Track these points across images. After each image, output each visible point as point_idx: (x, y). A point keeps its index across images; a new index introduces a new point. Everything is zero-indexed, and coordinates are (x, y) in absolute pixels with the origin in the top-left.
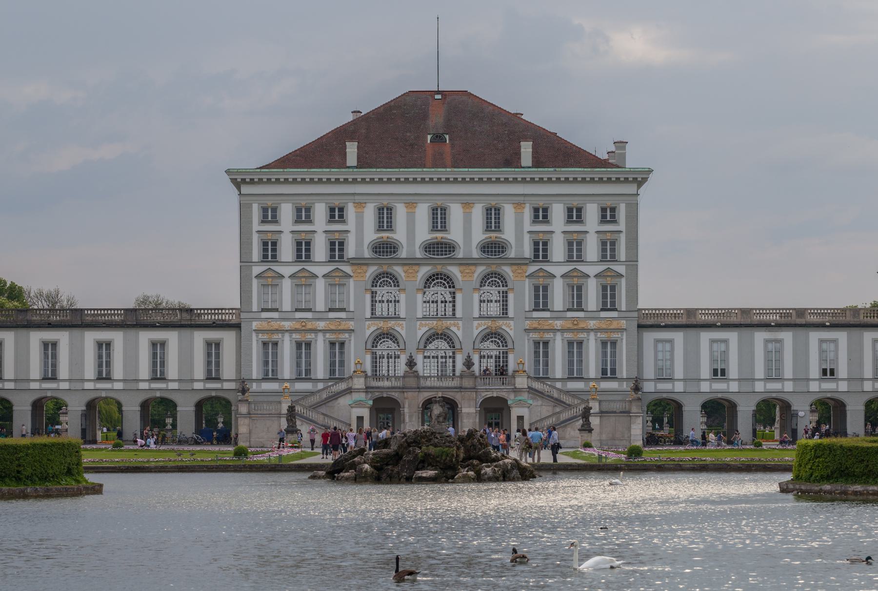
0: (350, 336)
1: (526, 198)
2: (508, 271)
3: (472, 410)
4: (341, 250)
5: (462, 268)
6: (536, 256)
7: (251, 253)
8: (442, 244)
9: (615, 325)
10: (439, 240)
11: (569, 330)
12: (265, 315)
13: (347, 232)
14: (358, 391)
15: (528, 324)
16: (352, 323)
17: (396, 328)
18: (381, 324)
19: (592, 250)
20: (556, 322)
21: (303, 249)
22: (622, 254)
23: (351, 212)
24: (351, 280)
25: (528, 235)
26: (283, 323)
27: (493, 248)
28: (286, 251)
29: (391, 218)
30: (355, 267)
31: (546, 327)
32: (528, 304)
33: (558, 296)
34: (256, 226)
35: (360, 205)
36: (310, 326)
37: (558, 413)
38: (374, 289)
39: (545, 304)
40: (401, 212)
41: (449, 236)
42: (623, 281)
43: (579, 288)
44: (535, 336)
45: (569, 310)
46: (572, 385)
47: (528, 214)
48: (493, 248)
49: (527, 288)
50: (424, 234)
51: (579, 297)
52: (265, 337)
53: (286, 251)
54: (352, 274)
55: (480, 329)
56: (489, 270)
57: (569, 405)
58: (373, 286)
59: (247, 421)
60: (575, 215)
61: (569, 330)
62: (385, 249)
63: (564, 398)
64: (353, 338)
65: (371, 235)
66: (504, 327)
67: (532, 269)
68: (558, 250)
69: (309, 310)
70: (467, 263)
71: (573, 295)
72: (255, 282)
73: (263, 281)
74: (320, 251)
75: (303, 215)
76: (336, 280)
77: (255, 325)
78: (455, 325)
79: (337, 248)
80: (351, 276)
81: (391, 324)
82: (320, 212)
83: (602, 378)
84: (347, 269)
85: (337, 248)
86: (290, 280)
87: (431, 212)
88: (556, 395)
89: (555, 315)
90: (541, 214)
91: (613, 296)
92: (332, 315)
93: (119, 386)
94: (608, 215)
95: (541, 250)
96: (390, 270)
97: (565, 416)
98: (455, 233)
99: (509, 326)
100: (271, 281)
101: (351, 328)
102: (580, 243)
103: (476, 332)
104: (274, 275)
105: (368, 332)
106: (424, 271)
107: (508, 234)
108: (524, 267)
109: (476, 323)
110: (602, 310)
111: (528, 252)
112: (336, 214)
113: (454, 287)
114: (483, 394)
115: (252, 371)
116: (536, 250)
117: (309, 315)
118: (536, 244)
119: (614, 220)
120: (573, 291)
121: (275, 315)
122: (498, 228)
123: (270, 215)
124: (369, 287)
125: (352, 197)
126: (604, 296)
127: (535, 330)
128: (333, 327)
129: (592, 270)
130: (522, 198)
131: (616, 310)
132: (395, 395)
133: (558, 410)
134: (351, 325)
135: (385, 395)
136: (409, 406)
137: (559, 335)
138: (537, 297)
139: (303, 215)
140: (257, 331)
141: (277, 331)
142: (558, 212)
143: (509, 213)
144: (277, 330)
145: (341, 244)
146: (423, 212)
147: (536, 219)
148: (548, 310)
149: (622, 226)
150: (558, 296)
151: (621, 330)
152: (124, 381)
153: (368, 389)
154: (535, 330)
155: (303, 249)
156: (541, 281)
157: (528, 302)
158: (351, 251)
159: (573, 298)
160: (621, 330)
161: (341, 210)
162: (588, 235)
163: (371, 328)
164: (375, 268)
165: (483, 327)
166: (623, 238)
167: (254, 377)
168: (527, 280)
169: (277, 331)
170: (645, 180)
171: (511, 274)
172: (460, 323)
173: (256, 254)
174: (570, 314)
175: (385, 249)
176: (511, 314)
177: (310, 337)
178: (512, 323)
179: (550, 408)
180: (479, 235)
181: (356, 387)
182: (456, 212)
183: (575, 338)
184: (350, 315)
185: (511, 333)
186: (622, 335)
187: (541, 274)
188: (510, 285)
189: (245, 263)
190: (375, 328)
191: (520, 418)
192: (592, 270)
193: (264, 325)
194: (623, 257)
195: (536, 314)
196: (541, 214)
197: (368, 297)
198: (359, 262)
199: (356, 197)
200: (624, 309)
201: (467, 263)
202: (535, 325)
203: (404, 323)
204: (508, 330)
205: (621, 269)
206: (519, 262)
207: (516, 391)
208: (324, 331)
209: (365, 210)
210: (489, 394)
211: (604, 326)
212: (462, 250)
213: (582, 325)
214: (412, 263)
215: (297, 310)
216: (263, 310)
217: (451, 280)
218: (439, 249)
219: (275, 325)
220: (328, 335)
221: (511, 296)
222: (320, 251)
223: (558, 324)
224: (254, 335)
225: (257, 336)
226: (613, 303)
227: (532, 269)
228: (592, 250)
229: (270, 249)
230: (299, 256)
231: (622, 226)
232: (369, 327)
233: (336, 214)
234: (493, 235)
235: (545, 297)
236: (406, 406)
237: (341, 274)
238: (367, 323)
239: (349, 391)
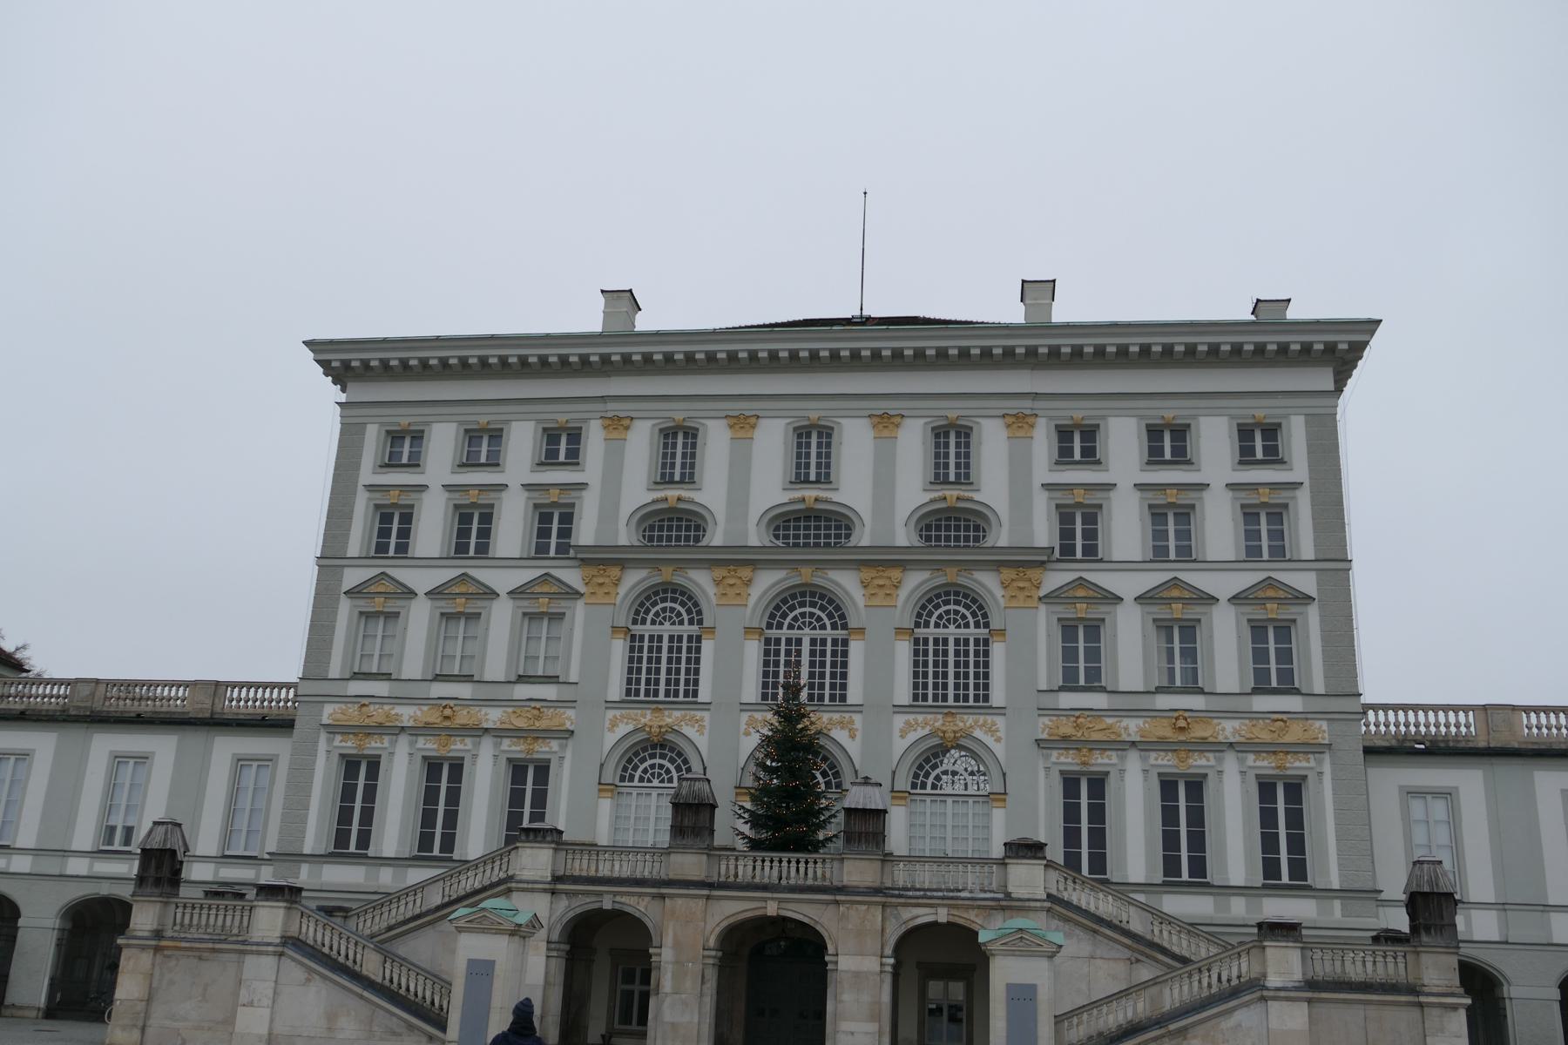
0: (563, 747)
1: (1039, 404)
2: (988, 583)
3: (871, 964)
4: (565, 533)
5: (867, 574)
6: (1067, 550)
7: (347, 536)
8: (818, 518)
9: (1295, 734)
10: (810, 503)
11: (1161, 745)
12: (357, 688)
13: (582, 486)
14: (530, 887)
15: (1043, 727)
16: (570, 713)
17: (687, 730)
18: (647, 717)
19: (1219, 529)
20: (1125, 722)
21: (472, 526)
22: (1304, 542)
23: (595, 440)
24: (580, 605)
25: (1045, 494)
26: (398, 710)
27: (952, 524)
28: (432, 529)
29: (693, 455)
30: (592, 571)
31: (1096, 736)
32: (1046, 670)
33: (1130, 649)
34: (367, 474)
35: (618, 425)
36: (462, 717)
37: (1145, 985)
38: (638, 629)
39: (1094, 674)
40: (716, 440)
41: (835, 497)
42: (1313, 614)
43: (1189, 630)
44: (1069, 760)
45: (1159, 690)
46: (1174, 904)
47: (1042, 441)
48: (952, 524)
49: (1042, 626)
50: (770, 487)
51: (1190, 654)
52: (349, 745)
53: (432, 529)
54: (582, 589)
55: (912, 737)
56: (941, 580)
57: (1185, 961)
58: (635, 622)
59: (146, 959)
60: (1168, 441)
61: (1161, 745)
62: (672, 526)
63: (1167, 938)
64: (568, 755)
65: (637, 491)
66: (978, 733)
67: (1055, 579)
68: (1126, 530)
69: (467, 678)
70: (883, 562)
71: (1170, 652)
72: (345, 608)
73: (364, 605)
74: (512, 529)
75: (482, 443)
76: (543, 607)
77: (328, 712)
78: (842, 725)
79: (553, 521)
80: (579, 595)
81: (672, 717)
82: (522, 441)
83: (1265, 887)
84: (572, 576)
85: (553, 521)
86: (429, 603)
87: (793, 440)
88: (1136, 926)
89: (1119, 702)
90: (1077, 443)
91: (1285, 656)
92: (523, 691)
93: (21, 864)
94: (1258, 441)
95: (1080, 526)
96: (678, 580)
97: (1174, 995)
98: (852, 487)
99: (992, 731)
100: (381, 606)
101: (568, 726)
102: (1185, 514)
103: (900, 745)
104: (391, 588)
105: (611, 739)
106: (766, 583)
107: (992, 486)
108: (1033, 573)
109: (899, 721)
110: (1256, 691)
111: (1043, 533)
112: (562, 444)
113: (845, 627)
114: (907, 913)
115: (303, 832)
116: (1067, 534)
117: (464, 690)
118: (1065, 518)
119: (1273, 456)
120: (1170, 640)
121: (380, 688)
122: (965, 477)
123: (404, 445)
124: (623, 620)
125: (599, 406)
126: (1260, 656)
127: (1065, 742)
128: (521, 723)
129: (1224, 585)
130: (1028, 403)
131: (1297, 692)
132: (639, 904)
133: (1145, 973)
134: (569, 718)
135: (607, 904)
136: (677, 945)
137: (1133, 758)
138: (1069, 655)
139: (482, 443)
140: (332, 729)
141: (381, 729)
142: (1123, 441)
143: (992, 442)
144: (381, 726)
145: (567, 518)
146: (772, 442)
147: (1064, 456)
148: (1103, 690)
149: (1299, 469)
150: (1130, 649)
151: (1313, 748)
152: (37, 852)
153: (558, 883)
154: (1065, 742)
155: (472, 526)
156: (1081, 610)
157: (1045, 666)
158: (586, 533)
159: (1171, 659)
160: (1313, 748)
161: (575, 437)
162: (1205, 494)
163: (617, 730)
164: (643, 573)
165: (921, 733)
166: (1303, 505)
167: (307, 851)
168: (1043, 609)
169: (381, 729)
170: (1358, 349)
171: (999, 592)
172: (857, 718)
173: (357, 542)
174: (1164, 702)
175: (672, 526)
176: (997, 697)
177: (459, 747)
178: (1000, 722)
179: (1121, 968)
180: (913, 491)
181: (527, 874)
182: (855, 442)
183: (1182, 769)
184: (567, 692)
185: (999, 749)
186: (1320, 762)
187: (1081, 593)
188: (995, 623)
189: (331, 560)
190: (630, 728)
191: (1023, 996)
192: (1224, 585)
193: (352, 714)
194: (1307, 550)
195: (1068, 700)
196: (1077, 443)
197: (619, 648)
198: (602, 560)
199: (611, 406)
200: (1319, 688)
201: (881, 563)
202: (1067, 729)
203: (706, 715)
204: (988, 740)
205: (1305, 582)
206: (1023, 562)
207: (1007, 904)
208: (499, 733)
209: (631, 435)
210: (924, 916)
211: (1266, 736)
212: (867, 529)
213: (1198, 732)
214: (736, 561)
215: (438, 678)
216: (357, 676)
217: (838, 608)
218: (812, 527)
219: (377, 713)
220: (506, 744)
221: (997, 650)
222: (512, 529)
223: (1132, 728)
224: (323, 737)
225: (330, 741)
226: (1286, 676)
227: (1055, 579)
228: (1219, 529)
229: (393, 526)
230: (461, 549)
231: (1299, 469)
232: (614, 725)
233: (562, 444)
234: (952, 493)
235: (1093, 655)
236: (668, 940)
237: (554, 589)
238: (610, 714)
239: (505, 886)
